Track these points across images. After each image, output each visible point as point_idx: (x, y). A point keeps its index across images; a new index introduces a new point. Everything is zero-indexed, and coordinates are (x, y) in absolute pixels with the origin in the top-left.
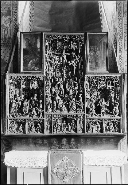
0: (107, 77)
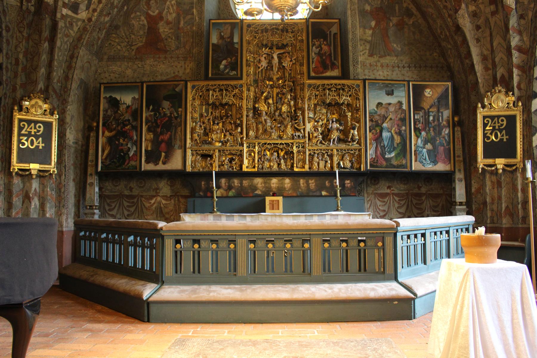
0: (339, 85)
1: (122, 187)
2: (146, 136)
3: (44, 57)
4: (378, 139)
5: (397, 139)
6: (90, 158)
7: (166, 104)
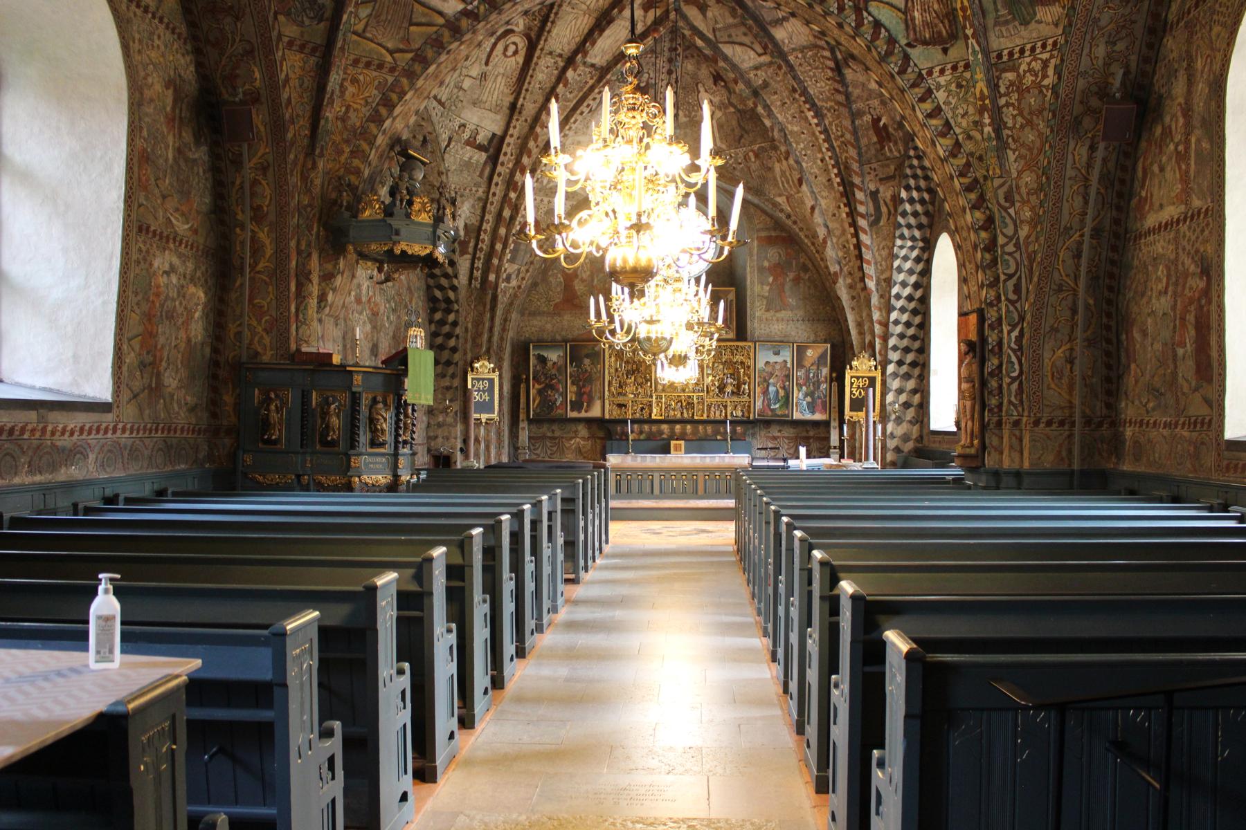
1: (545, 429)
2: (572, 389)
3: (487, 325)
4: (765, 392)
5: (782, 393)
6: (521, 406)
7: (587, 361)
